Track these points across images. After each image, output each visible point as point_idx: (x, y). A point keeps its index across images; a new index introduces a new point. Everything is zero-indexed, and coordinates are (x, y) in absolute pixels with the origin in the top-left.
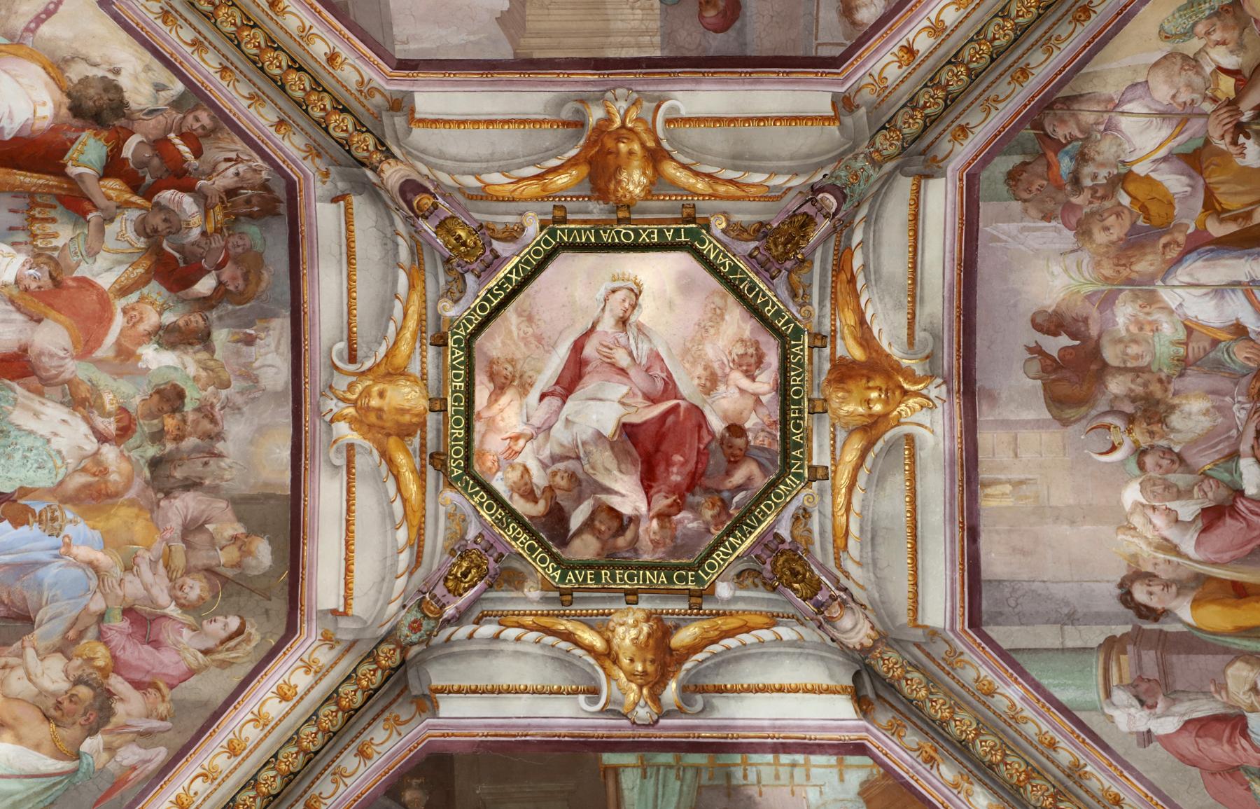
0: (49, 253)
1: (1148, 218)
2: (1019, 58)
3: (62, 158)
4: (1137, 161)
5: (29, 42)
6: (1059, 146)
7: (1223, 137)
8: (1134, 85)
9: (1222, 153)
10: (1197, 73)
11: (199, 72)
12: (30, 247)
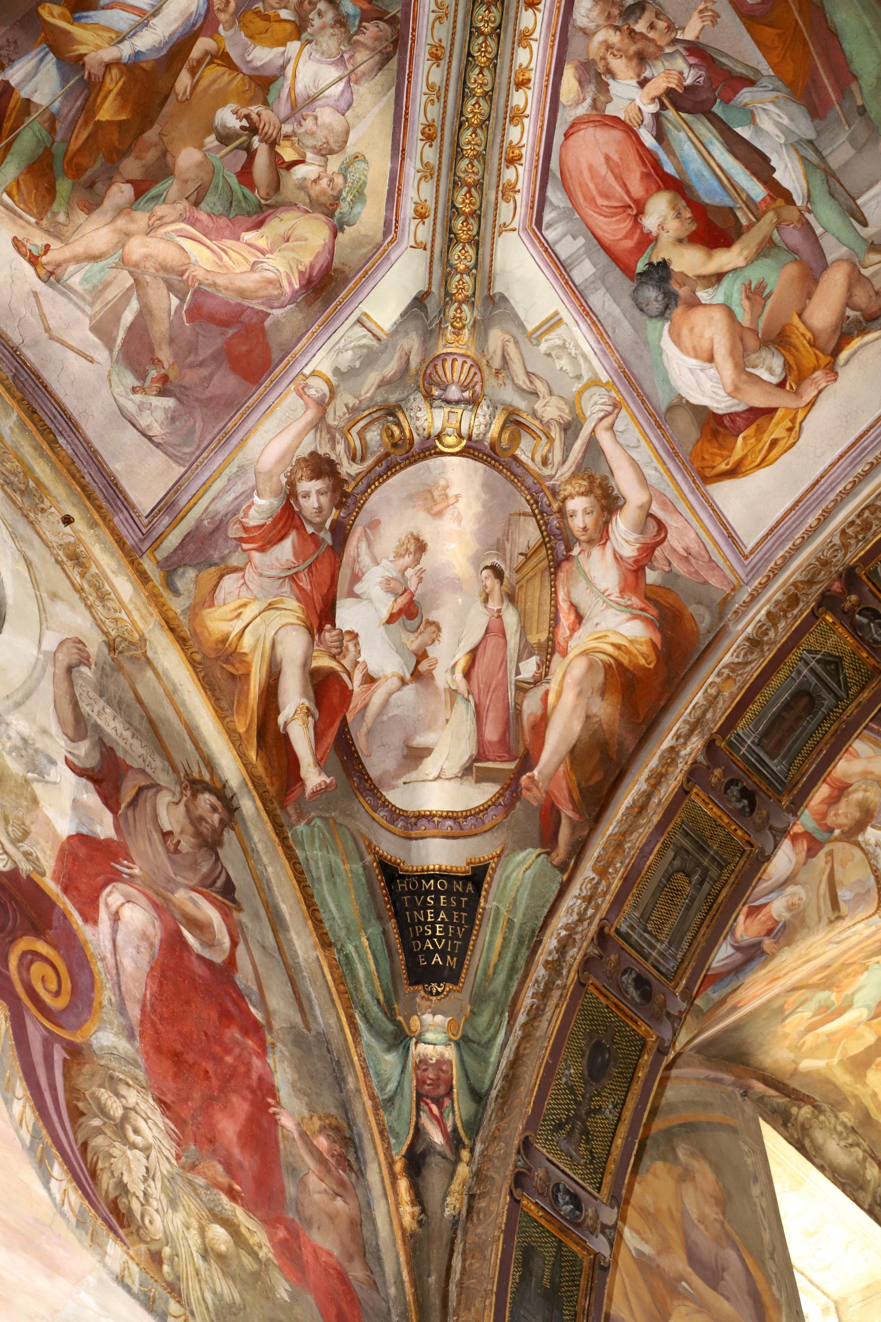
1: (257, 13)
2: (449, 68)
4: (301, 50)
6: (365, 17)
7: (259, 115)
8: (350, 106)
9: (250, 102)
10: (314, 147)
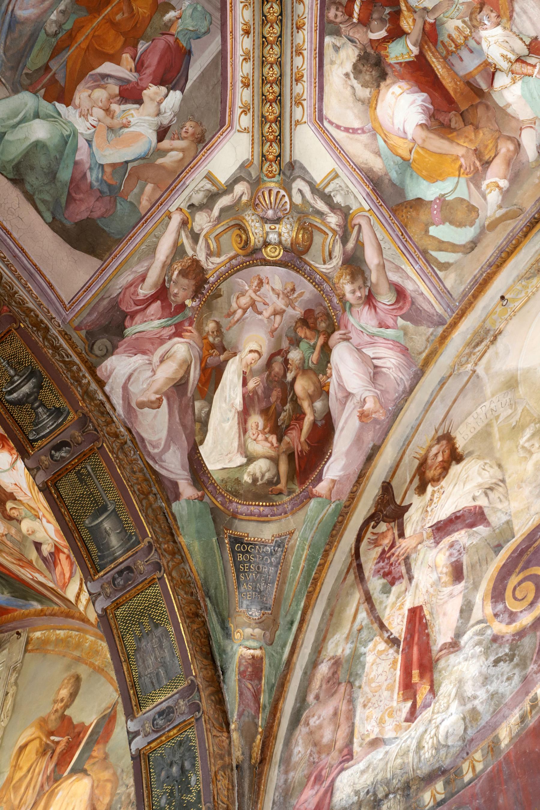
0: (469, 23)
3: (413, 61)
5: (369, 126)
11: (311, 38)
12: (474, 34)
